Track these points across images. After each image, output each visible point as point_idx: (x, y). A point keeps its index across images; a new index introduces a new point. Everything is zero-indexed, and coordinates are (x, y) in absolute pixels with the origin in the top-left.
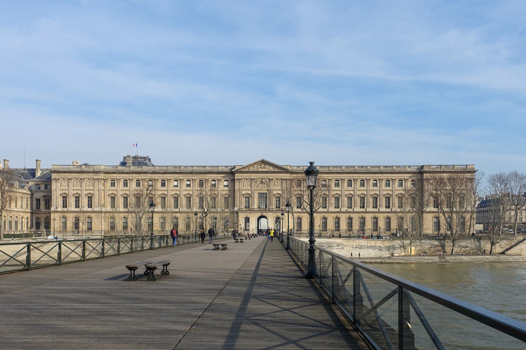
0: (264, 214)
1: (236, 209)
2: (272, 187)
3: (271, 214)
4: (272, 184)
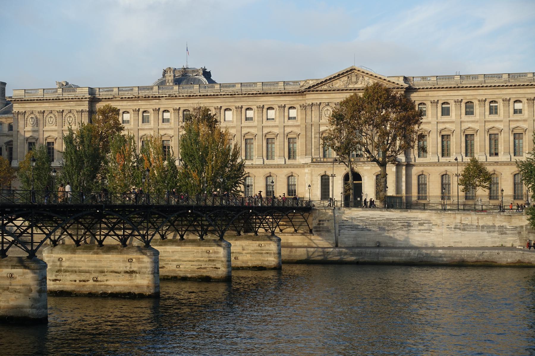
3: (369, 168)
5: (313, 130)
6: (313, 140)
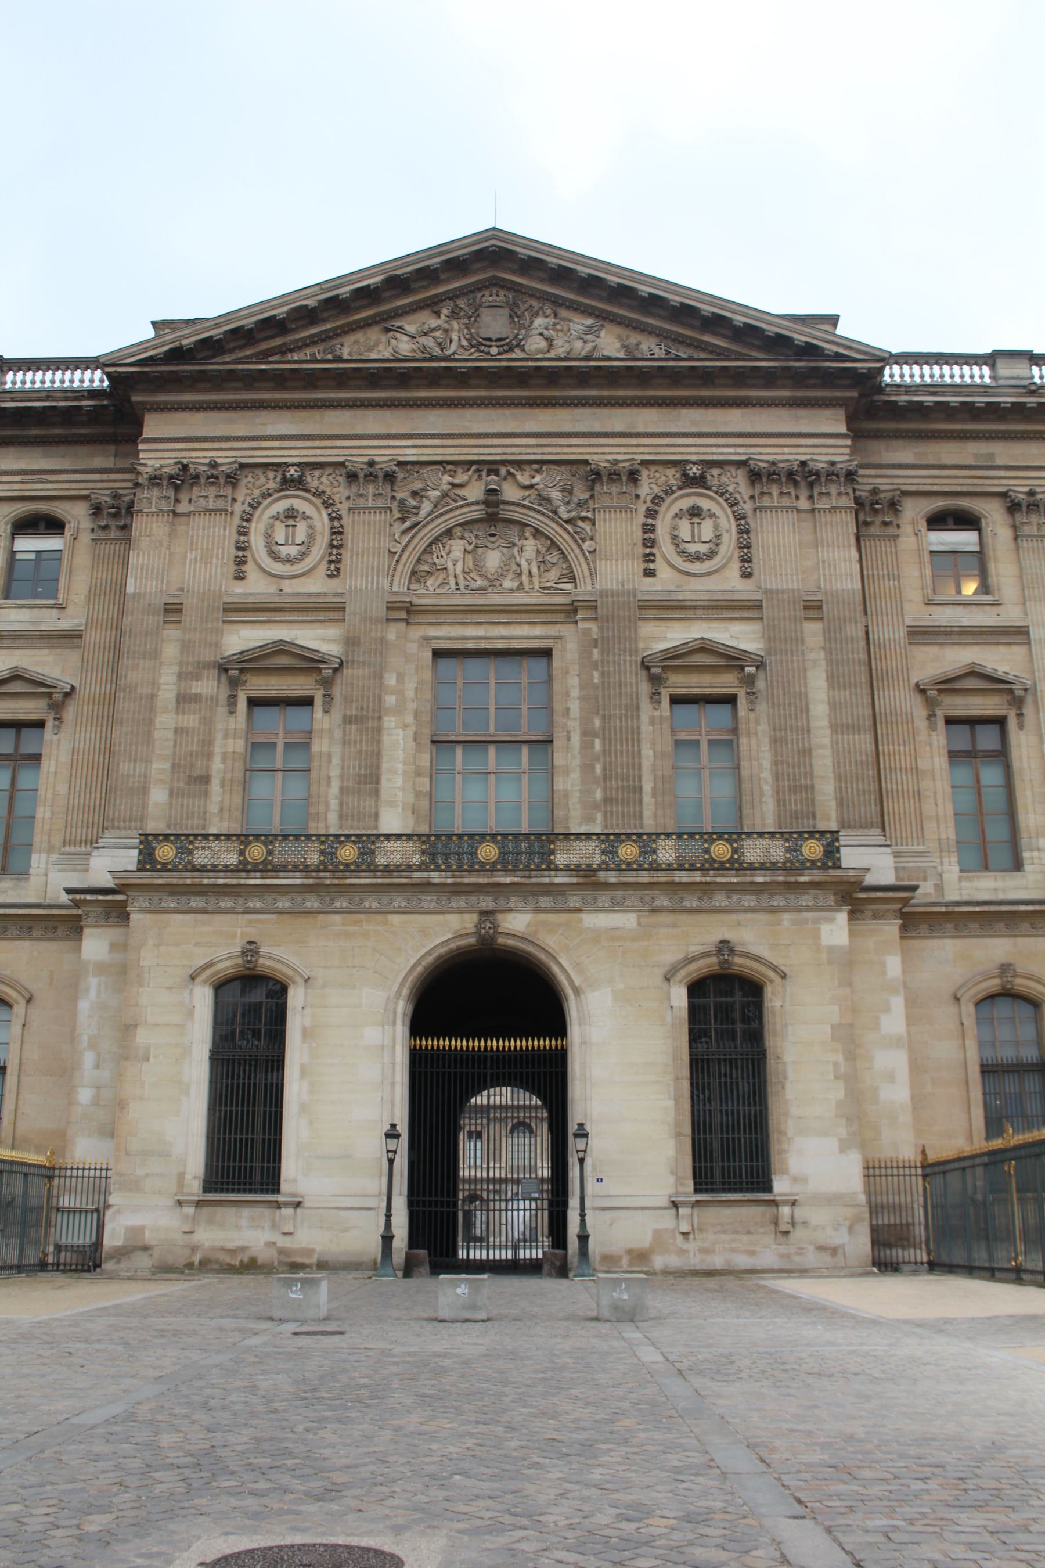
0: (518, 923)
1: (109, 863)
3: (626, 920)
4: (616, 530)
5: (170, 651)
6: (166, 721)
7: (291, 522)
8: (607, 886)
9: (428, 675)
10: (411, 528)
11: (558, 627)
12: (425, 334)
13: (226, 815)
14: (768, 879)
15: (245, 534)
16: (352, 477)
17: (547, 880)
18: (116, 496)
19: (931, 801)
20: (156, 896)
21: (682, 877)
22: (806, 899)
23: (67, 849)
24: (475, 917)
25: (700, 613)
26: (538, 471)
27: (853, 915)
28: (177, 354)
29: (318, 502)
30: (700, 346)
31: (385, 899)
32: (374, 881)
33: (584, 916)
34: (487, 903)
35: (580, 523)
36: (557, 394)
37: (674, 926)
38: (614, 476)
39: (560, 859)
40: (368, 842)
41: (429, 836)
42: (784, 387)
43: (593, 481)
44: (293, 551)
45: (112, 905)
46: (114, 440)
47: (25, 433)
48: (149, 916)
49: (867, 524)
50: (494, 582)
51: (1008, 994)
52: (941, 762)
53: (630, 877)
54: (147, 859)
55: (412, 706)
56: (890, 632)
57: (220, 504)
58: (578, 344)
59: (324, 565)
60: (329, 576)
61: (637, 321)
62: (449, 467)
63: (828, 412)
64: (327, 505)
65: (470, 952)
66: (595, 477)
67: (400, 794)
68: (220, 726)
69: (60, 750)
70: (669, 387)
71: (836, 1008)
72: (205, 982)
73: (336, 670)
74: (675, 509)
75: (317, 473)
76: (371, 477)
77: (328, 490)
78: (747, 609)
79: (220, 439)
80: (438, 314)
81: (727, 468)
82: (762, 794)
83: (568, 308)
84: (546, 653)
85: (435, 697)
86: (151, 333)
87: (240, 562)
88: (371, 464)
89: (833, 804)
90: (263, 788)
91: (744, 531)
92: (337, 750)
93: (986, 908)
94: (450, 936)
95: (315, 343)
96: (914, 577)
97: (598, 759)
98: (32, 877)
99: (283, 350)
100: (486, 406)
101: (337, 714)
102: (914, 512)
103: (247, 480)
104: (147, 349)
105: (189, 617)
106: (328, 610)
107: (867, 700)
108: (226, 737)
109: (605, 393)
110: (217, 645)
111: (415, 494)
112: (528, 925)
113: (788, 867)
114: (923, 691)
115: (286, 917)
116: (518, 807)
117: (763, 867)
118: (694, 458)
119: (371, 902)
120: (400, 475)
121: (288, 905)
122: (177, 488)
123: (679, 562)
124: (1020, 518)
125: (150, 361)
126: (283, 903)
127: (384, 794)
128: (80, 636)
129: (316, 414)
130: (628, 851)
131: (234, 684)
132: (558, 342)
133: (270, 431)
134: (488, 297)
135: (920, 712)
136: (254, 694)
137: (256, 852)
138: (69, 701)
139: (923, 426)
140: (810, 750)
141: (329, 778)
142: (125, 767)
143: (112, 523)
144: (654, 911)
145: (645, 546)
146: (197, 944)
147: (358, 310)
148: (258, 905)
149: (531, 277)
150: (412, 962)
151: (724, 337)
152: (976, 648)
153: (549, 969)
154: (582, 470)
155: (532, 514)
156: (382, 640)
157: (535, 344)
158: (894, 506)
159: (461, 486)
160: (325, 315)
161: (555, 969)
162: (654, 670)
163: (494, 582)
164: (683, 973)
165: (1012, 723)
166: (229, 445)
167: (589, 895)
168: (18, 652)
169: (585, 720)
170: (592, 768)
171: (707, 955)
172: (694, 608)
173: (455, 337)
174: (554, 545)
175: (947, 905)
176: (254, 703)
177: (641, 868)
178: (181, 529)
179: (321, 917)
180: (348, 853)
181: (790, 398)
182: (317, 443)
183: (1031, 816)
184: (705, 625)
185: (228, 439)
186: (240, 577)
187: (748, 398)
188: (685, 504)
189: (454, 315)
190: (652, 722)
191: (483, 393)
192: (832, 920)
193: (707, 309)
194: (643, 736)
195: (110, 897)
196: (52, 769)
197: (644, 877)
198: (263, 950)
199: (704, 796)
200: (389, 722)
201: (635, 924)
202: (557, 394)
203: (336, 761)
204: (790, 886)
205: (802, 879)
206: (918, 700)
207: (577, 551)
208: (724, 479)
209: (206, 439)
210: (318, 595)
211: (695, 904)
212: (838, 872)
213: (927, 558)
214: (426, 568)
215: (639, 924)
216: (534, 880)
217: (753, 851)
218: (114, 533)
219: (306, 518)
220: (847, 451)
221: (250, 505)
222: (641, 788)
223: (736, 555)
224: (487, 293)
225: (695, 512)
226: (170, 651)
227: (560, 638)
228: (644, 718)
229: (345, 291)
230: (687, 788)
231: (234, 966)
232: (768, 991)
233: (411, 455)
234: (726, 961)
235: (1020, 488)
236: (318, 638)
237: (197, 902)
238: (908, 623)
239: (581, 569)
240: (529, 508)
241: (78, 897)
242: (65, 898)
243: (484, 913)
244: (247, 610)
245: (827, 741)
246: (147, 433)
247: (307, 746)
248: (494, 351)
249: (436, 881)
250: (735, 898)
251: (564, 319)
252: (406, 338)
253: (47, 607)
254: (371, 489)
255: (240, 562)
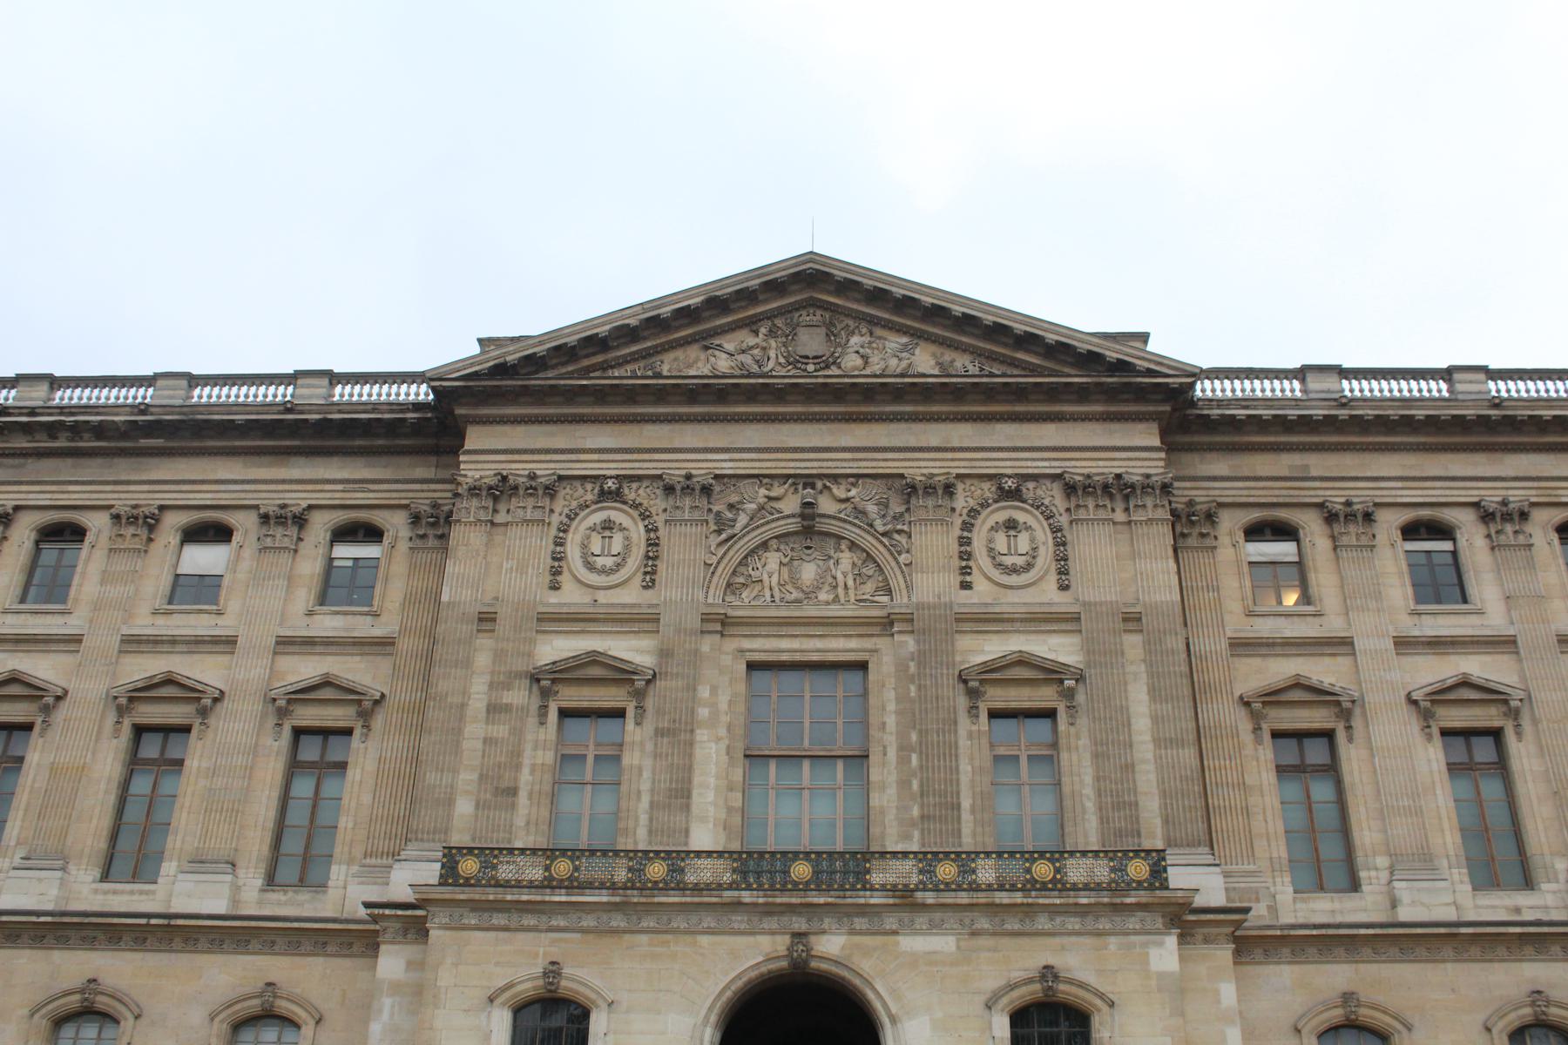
0: (832, 947)
1: (411, 876)
2: (932, 584)
3: (944, 944)
4: (933, 543)
5: (482, 660)
6: (475, 730)
7: (607, 533)
8: (924, 907)
9: (741, 687)
10: (727, 540)
11: (874, 640)
12: (743, 352)
13: (533, 829)
14: (1092, 900)
15: (561, 545)
16: (669, 490)
17: (862, 901)
18: (435, 506)
19: (1261, 817)
20: (457, 911)
21: (1003, 898)
22: (1133, 922)
23: (368, 861)
24: (787, 939)
25: (1017, 625)
26: (853, 485)
27: (1183, 939)
28: (501, 370)
29: (635, 514)
30: (1013, 363)
31: (694, 919)
32: (684, 900)
33: (900, 938)
34: (799, 924)
35: (896, 536)
36: (872, 409)
37: (995, 950)
38: (930, 490)
39: (876, 878)
40: (677, 858)
41: (740, 853)
42: (1097, 401)
43: (909, 494)
44: (609, 562)
45: (411, 920)
46: (436, 451)
47: (350, 443)
48: (448, 933)
49: (1183, 535)
50: (809, 595)
51: (1352, 1025)
52: (1269, 777)
53: (948, 898)
54: (450, 874)
55: (725, 719)
56: (1211, 644)
57: (538, 515)
58: (893, 362)
59: (639, 576)
60: (645, 587)
61: (952, 340)
62: (766, 481)
63: (1141, 426)
64: (644, 517)
65: (782, 976)
66: (911, 490)
67: (712, 809)
68: (529, 737)
69: (366, 759)
70: (984, 403)
71: (1169, 1039)
72: (503, 1004)
73: (649, 682)
74: (991, 522)
75: (634, 485)
76: (688, 490)
77: (645, 502)
78: (1067, 621)
79: (539, 451)
80: (756, 333)
81: (1042, 481)
82: (1084, 811)
83: (884, 327)
84: (862, 666)
85: (749, 710)
86: (476, 350)
87: (556, 572)
88: (689, 477)
89: (1158, 822)
90: (571, 801)
91: (1061, 544)
92: (648, 763)
93: (1323, 932)
94: (761, 959)
95: (636, 360)
96: (1233, 588)
97: (914, 775)
98: (331, 891)
99: (604, 367)
100: (803, 421)
101: (649, 726)
102: (1230, 524)
103: (564, 491)
104: (472, 365)
105: (504, 626)
106: (641, 621)
107: (1190, 713)
108: (535, 748)
109: (921, 408)
110: (530, 655)
111: (731, 506)
112: (843, 948)
113: (1113, 888)
114: (1247, 704)
115: (591, 937)
116: (833, 825)
117: (1086, 887)
118: (1009, 471)
119: (679, 922)
120: (717, 488)
121: (593, 923)
122: (496, 499)
123: (996, 574)
124: (1337, 528)
125: (475, 376)
126: (589, 921)
127: (695, 809)
128: (393, 644)
129: (635, 429)
130: (946, 871)
131: (545, 694)
132: (874, 359)
133: (589, 444)
134: (805, 317)
135: (1245, 726)
136: (565, 704)
137: (563, 867)
138: (377, 709)
139: (1237, 439)
140: (1133, 765)
141: (639, 792)
142: (431, 777)
143: (431, 532)
144: (974, 934)
145: (961, 558)
146: (497, 964)
147: (678, 329)
148: (562, 923)
149: (847, 298)
150: (722, 986)
151: (1037, 354)
152: (1300, 660)
153: (864, 995)
154: (898, 483)
155: (848, 526)
156: (696, 651)
157: (851, 361)
158: (1210, 517)
159: (777, 499)
160: (646, 333)
161: (871, 995)
162: (972, 684)
163: (809, 595)
164: (1005, 1000)
165: (1341, 736)
166: (549, 457)
167: (906, 916)
168: (330, 658)
169: (902, 735)
170: (910, 783)
171: (1030, 981)
172: (1012, 620)
173: (772, 354)
174: (869, 557)
175: (1282, 928)
176: (564, 713)
177: (959, 889)
178: (498, 539)
179: (627, 937)
180: (657, 870)
181: (1103, 413)
182: (635, 456)
183: (1366, 833)
184: (1022, 637)
185: (547, 451)
186: (555, 587)
187: (1062, 413)
188: (1001, 517)
189: (772, 333)
190: (970, 736)
191: (799, 409)
192: (1161, 944)
193: (1019, 328)
194: (961, 751)
195: (409, 913)
196: (358, 778)
197: (963, 898)
198: (566, 971)
199: (1024, 813)
200: (702, 735)
201: (954, 949)
202: (872, 409)
203: (646, 774)
204: (1117, 908)
205: (1128, 900)
206: (1242, 713)
207: (893, 564)
208: (1039, 492)
209: (525, 451)
210: (633, 606)
211: (1017, 927)
212: (1165, 893)
213: (1246, 568)
214: (741, 580)
215: (958, 947)
216: (849, 901)
217: (1077, 871)
218: (431, 542)
219: (622, 529)
220: (1162, 463)
221: (568, 516)
222: (959, 805)
223: (1053, 567)
224: (804, 313)
225: (1011, 525)
226: (482, 660)
227: (876, 651)
228: (962, 733)
229: (666, 311)
230: (1007, 805)
231: (535, 988)
232: (1096, 1021)
233: (727, 468)
234: (1050, 988)
235: (1336, 498)
236: (632, 649)
237: (499, 919)
238: (1229, 634)
239: (897, 582)
240: (845, 521)
241: (376, 911)
242: (362, 912)
243: (799, 936)
244: (560, 620)
245: (1150, 756)
246: (469, 444)
247: (617, 759)
248: (811, 368)
249: (747, 900)
250: (1058, 920)
251: (880, 338)
252: (724, 356)
253: (361, 614)
254: (688, 501)
255: (556, 572)
